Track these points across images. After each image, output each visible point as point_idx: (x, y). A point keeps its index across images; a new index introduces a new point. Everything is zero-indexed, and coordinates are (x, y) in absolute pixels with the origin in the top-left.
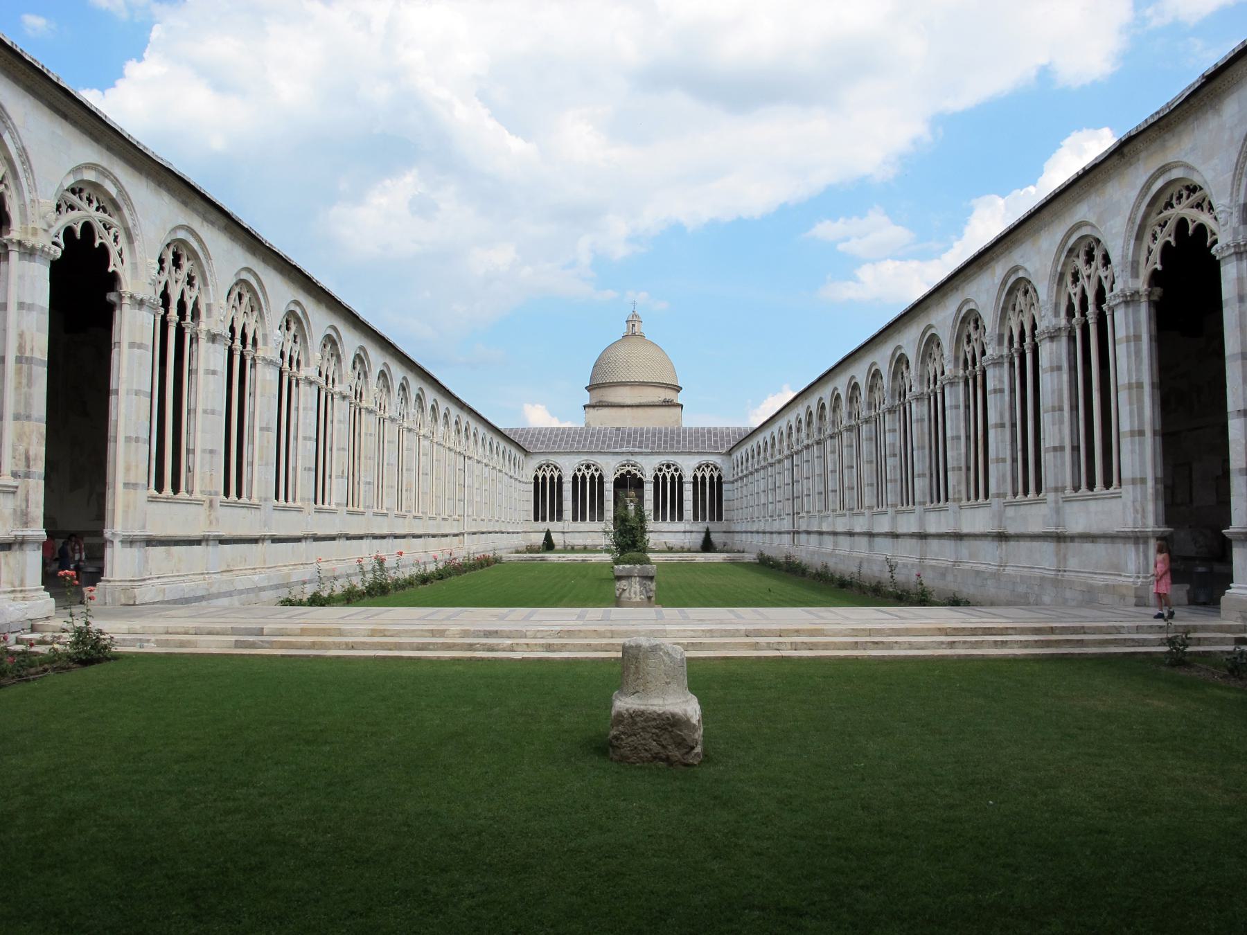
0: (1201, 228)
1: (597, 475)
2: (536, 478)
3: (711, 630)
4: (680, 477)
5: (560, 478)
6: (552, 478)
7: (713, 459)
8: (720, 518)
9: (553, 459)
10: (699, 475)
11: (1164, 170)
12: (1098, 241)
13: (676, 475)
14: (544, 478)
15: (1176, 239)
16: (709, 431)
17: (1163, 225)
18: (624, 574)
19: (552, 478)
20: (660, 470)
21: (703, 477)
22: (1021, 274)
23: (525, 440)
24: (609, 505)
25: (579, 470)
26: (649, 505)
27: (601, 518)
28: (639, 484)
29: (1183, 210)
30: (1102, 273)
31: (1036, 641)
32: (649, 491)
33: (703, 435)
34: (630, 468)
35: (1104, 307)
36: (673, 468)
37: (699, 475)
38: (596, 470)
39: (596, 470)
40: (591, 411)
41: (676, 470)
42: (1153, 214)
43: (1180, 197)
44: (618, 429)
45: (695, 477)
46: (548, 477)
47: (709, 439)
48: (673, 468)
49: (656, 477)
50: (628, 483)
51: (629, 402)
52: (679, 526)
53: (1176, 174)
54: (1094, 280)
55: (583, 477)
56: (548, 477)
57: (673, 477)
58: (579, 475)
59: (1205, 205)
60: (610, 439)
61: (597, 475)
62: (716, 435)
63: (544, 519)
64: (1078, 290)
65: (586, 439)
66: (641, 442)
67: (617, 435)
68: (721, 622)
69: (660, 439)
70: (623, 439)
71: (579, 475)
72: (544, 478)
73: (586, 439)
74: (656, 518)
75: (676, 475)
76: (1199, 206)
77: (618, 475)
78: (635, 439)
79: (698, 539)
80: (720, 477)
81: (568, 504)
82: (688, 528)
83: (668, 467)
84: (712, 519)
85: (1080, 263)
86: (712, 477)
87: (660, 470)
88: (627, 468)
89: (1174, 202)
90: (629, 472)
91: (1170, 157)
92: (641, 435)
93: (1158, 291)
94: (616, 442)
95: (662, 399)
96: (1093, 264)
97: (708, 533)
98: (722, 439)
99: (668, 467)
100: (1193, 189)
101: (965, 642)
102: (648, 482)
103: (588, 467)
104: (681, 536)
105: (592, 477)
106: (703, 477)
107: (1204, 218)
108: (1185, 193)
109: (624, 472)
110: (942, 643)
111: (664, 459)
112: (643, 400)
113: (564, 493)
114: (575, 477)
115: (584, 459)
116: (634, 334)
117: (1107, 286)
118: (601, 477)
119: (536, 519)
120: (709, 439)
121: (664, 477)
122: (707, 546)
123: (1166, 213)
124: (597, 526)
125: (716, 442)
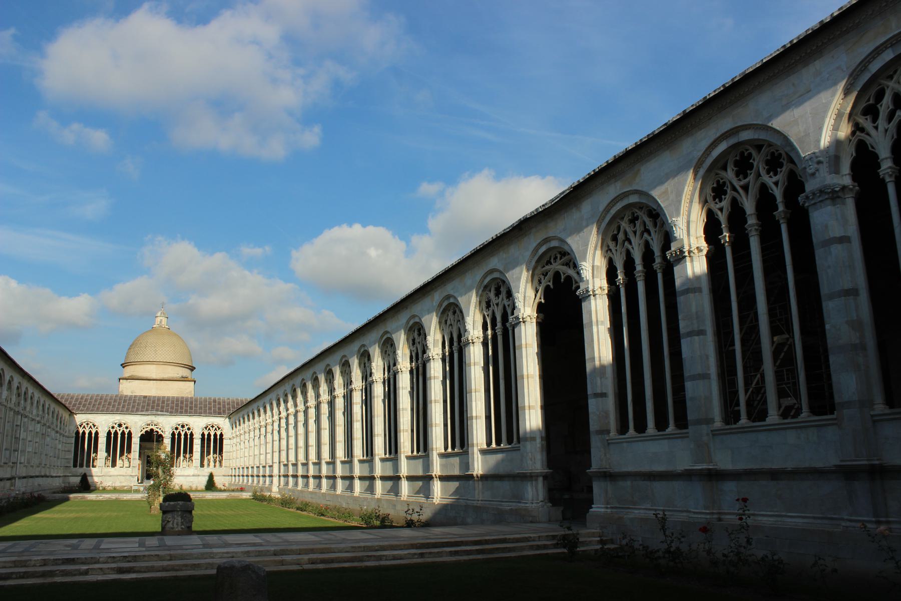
0: (569, 279)
1: (126, 431)
3: (248, 552)
4: (192, 434)
5: (97, 433)
6: (90, 433)
10: (206, 433)
11: (546, 240)
12: (504, 282)
13: (189, 433)
15: (553, 284)
16: (215, 401)
17: (545, 274)
18: (169, 509)
19: (90, 433)
20: (177, 429)
21: (209, 435)
22: (452, 300)
23: (70, 403)
25: (113, 427)
28: (160, 438)
29: (557, 266)
30: (506, 302)
31: (477, 550)
32: (167, 442)
33: (210, 403)
35: (508, 325)
36: (186, 427)
37: (206, 433)
38: (127, 428)
39: (127, 428)
41: (189, 429)
42: (539, 268)
43: (556, 258)
44: (145, 397)
45: (203, 435)
46: (87, 432)
47: (215, 406)
48: (186, 427)
49: (173, 434)
50: (150, 438)
51: (154, 377)
52: (191, 471)
53: (554, 244)
54: (501, 307)
55: (116, 433)
56: (87, 432)
57: (186, 434)
58: (113, 431)
59: (571, 264)
60: (139, 404)
61: (126, 431)
62: (219, 404)
63: (81, 466)
64: (490, 312)
65: (119, 404)
66: (163, 407)
67: (144, 402)
68: (254, 545)
69: (177, 405)
70: (148, 405)
71: (113, 431)
73: (119, 404)
75: (189, 433)
76: (567, 264)
77: (143, 432)
78: (158, 405)
79: (204, 480)
80: (221, 435)
82: (196, 472)
83: (183, 426)
85: (492, 295)
86: (215, 435)
87: (177, 429)
88: (151, 427)
89: (552, 260)
90: (152, 430)
91: (551, 234)
92: (163, 402)
93: (541, 315)
94: (143, 407)
95: (180, 375)
96: (501, 296)
97: (211, 476)
98: (224, 406)
99: (183, 426)
100: (564, 254)
101: (430, 553)
103: (120, 425)
104: (192, 479)
105: (123, 433)
106: (209, 435)
107: (571, 272)
108: (559, 256)
109: (148, 429)
110: (415, 554)
112: (166, 376)
113: (99, 446)
114: (109, 433)
117: (509, 312)
118: (130, 433)
119: (75, 466)
120: (215, 406)
121: (179, 434)
122: (211, 485)
123: (547, 267)
124: (124, 471)
125: (219, 409)
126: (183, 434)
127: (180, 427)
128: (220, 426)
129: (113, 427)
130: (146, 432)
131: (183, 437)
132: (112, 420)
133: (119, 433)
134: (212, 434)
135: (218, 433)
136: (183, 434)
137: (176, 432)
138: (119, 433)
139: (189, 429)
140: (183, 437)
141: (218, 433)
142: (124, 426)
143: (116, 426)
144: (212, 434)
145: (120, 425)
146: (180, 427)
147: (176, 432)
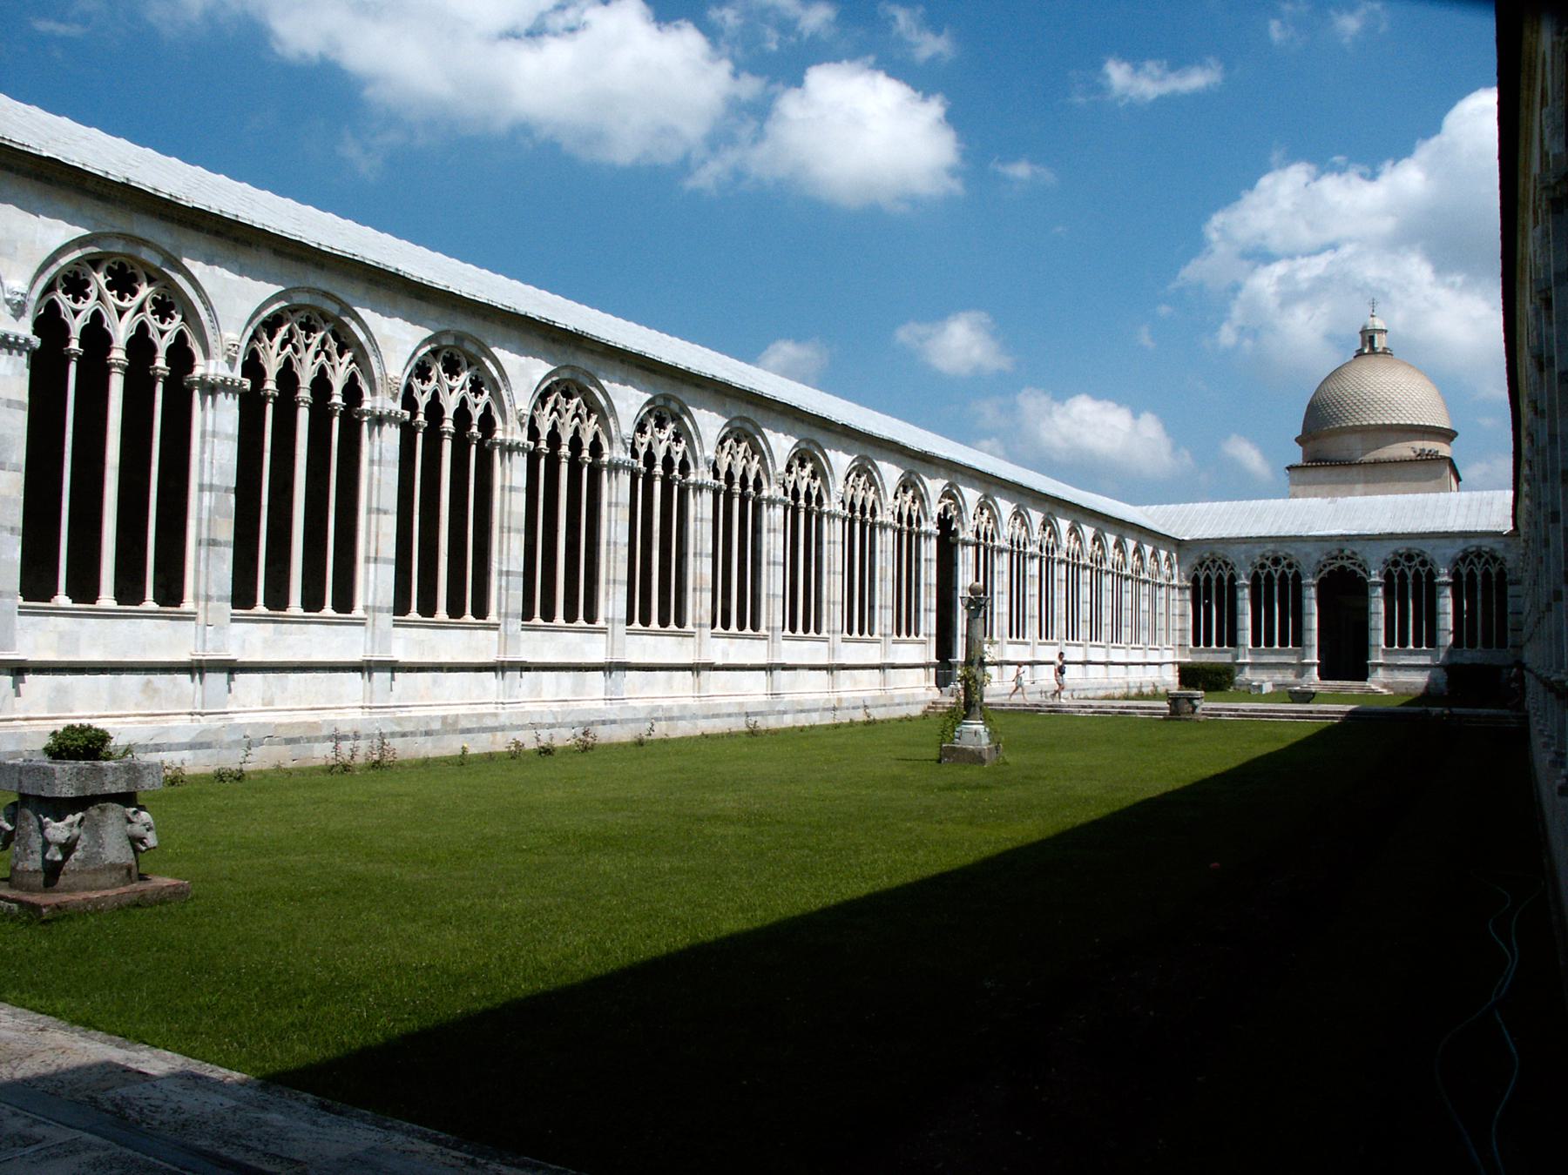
1: (1290, 573)
2: (1195, 580)
6: (1220, 579)
7: (1487, 545)
8: (1502, 644)
9: (1220, 551)
10: (1464, 571)
14: (1208, 579)
19: (1220, 579)
20: (1396, 563)
21: (1471, 575)
24: (1313, 622)
26: (1378, 622)
27: (1299, 641)
34: (1346, 563)
36: (1417, 560)
37: (1464, 571)
39: (1290, 566)
40: (1296, 475)
46: (1214, 578)
48: (1417, 560)
55: (1269, 577)
56: (1214, 578)
57: (1417, 575)
58: (1263, 573)
61: (1290, 573)
71: (1263, 573)
72: (1208, 579)
74: (1389, 642)
80: (1502, 574)
81: (1246, 621)
84: (1487, 644)
88: (1339, 563)
90: (1342, 568)
102: (1376, 584)
105: (1283, 576)
106: (1471, 575)
111: (1401, 547)
115: (1270, 546)
116: (1373, 350)
119: (1196, 643)
121: (1403, 576)
126: (1410, 574)
127: (1402, 560)
128: (1499, 555)
129: (1263, 566)
130: (1330, 572)
131: (1410, 580)
132: (1258, 551)
133: (1276, 576)
134: (1478, 573)
135: (1494, 570)
136: (1410, 574)
137: (1396, 572)
138: (1276, 576)
139: (1424, 563)
140: (1410, 580)
141: (1494, 570)
142: (1284, 563)
143: (1268, 563)
144: (1478, 573)
145: (1276, 561)
146: (1402, 560)
147: (1396, 572)
